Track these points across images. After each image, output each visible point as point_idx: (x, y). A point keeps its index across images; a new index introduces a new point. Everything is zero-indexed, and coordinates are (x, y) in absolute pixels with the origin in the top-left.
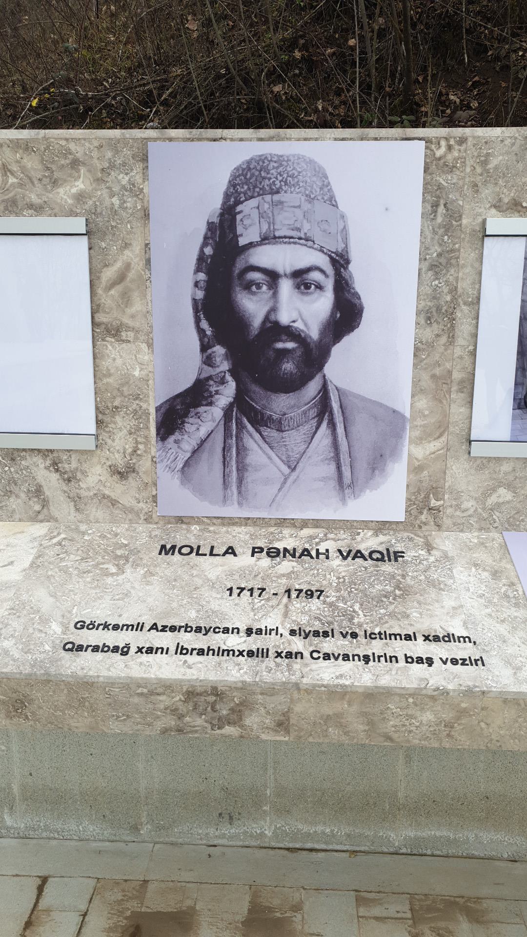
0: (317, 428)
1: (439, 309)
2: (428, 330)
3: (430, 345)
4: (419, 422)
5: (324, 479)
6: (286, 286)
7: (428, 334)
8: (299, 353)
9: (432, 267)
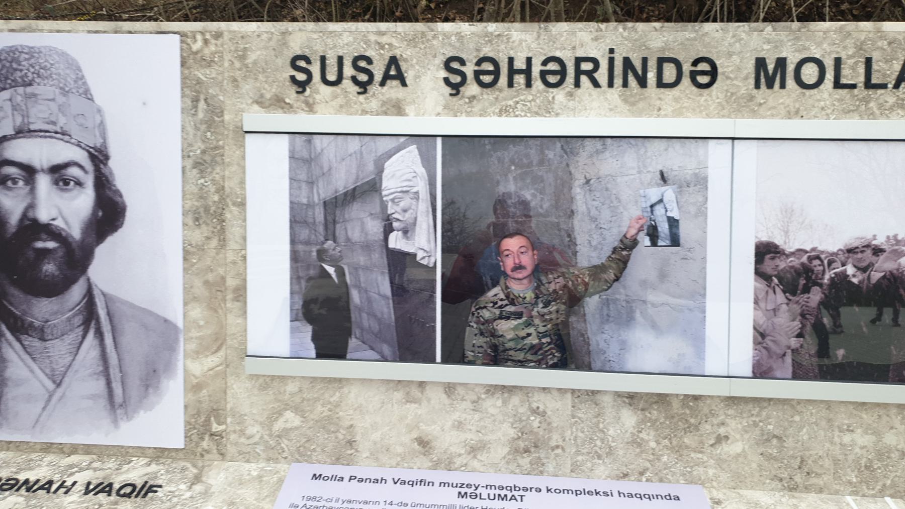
0: (84, 337)
1: (207, 209)
2: (197, 232)
3: (201, 248)
4: (194, 333)
5: (93, 397)
6: (43, 182)
7: (197, 236)
8: (60, 253)
9: (196, 165)
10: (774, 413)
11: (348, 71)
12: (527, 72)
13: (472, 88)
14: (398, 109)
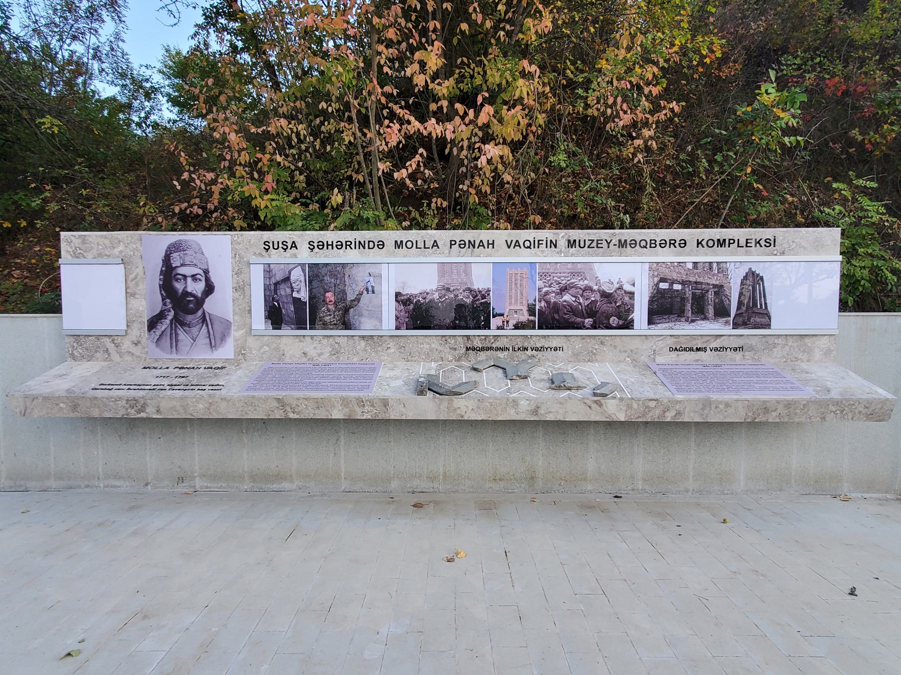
6: (189, 280)
7: (236, 295)
10: (402, 339)
11: (281, 245)
12: (332, 245)
13: (316, 250)
14: (295, 256)
